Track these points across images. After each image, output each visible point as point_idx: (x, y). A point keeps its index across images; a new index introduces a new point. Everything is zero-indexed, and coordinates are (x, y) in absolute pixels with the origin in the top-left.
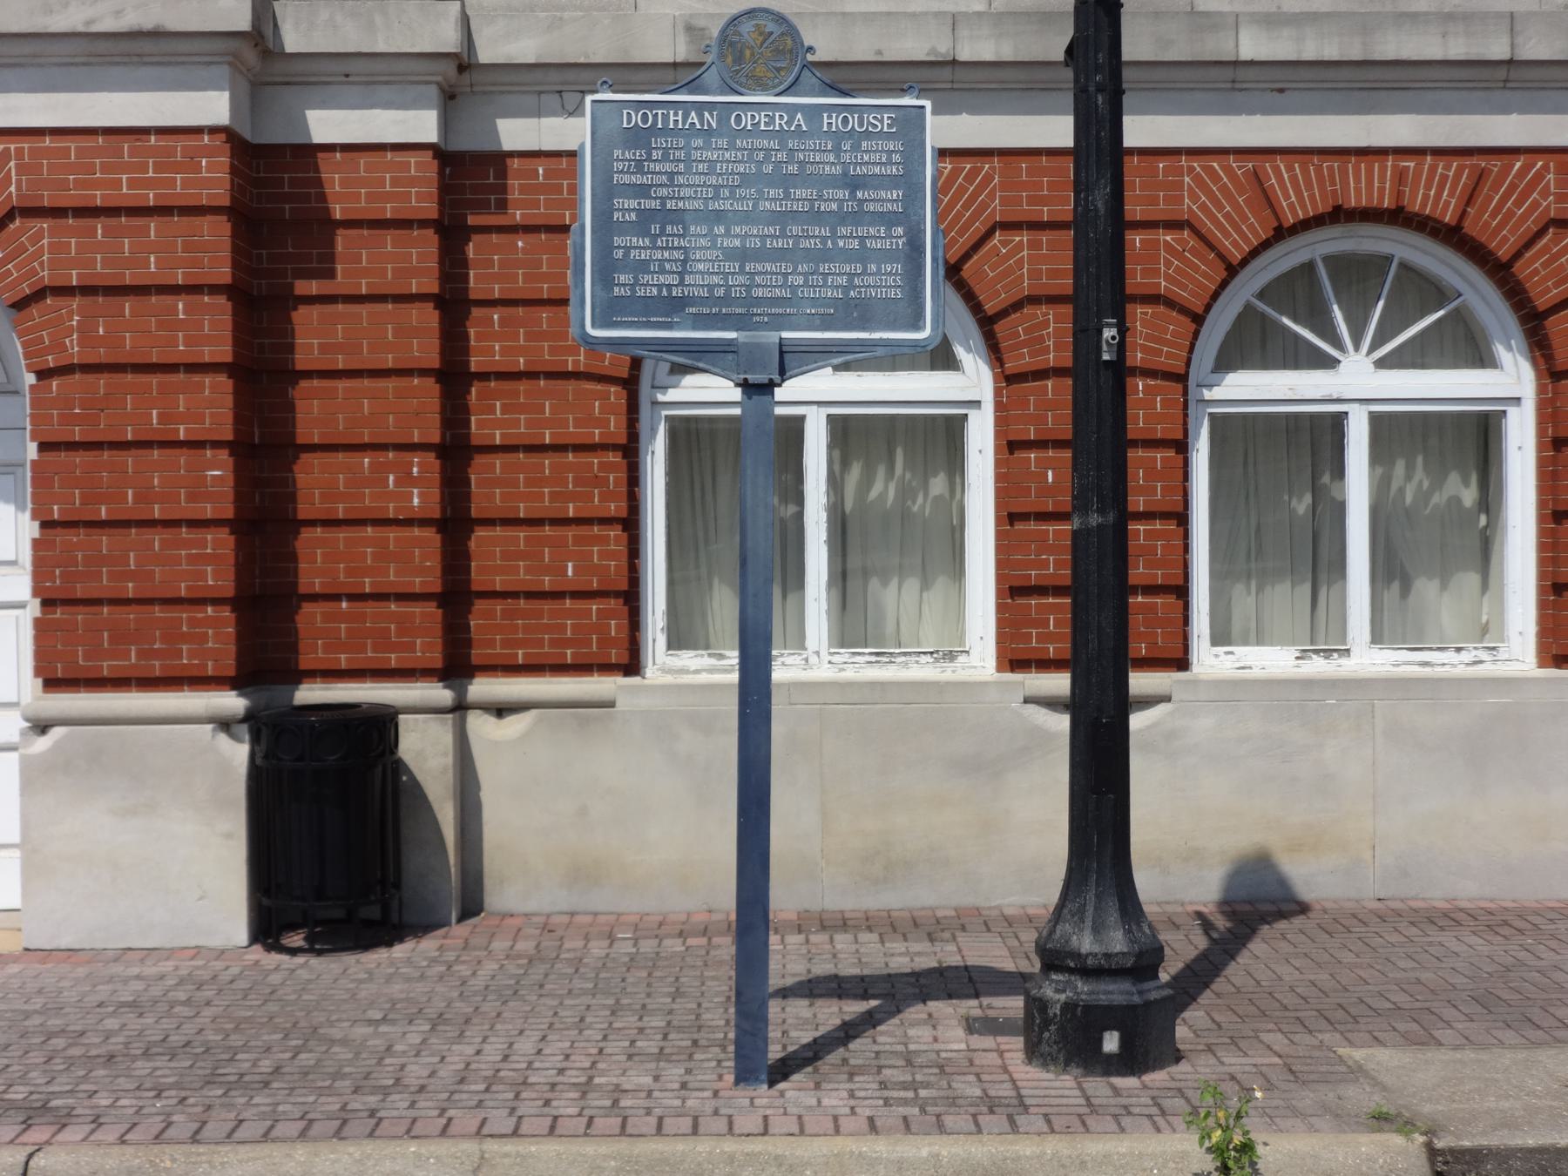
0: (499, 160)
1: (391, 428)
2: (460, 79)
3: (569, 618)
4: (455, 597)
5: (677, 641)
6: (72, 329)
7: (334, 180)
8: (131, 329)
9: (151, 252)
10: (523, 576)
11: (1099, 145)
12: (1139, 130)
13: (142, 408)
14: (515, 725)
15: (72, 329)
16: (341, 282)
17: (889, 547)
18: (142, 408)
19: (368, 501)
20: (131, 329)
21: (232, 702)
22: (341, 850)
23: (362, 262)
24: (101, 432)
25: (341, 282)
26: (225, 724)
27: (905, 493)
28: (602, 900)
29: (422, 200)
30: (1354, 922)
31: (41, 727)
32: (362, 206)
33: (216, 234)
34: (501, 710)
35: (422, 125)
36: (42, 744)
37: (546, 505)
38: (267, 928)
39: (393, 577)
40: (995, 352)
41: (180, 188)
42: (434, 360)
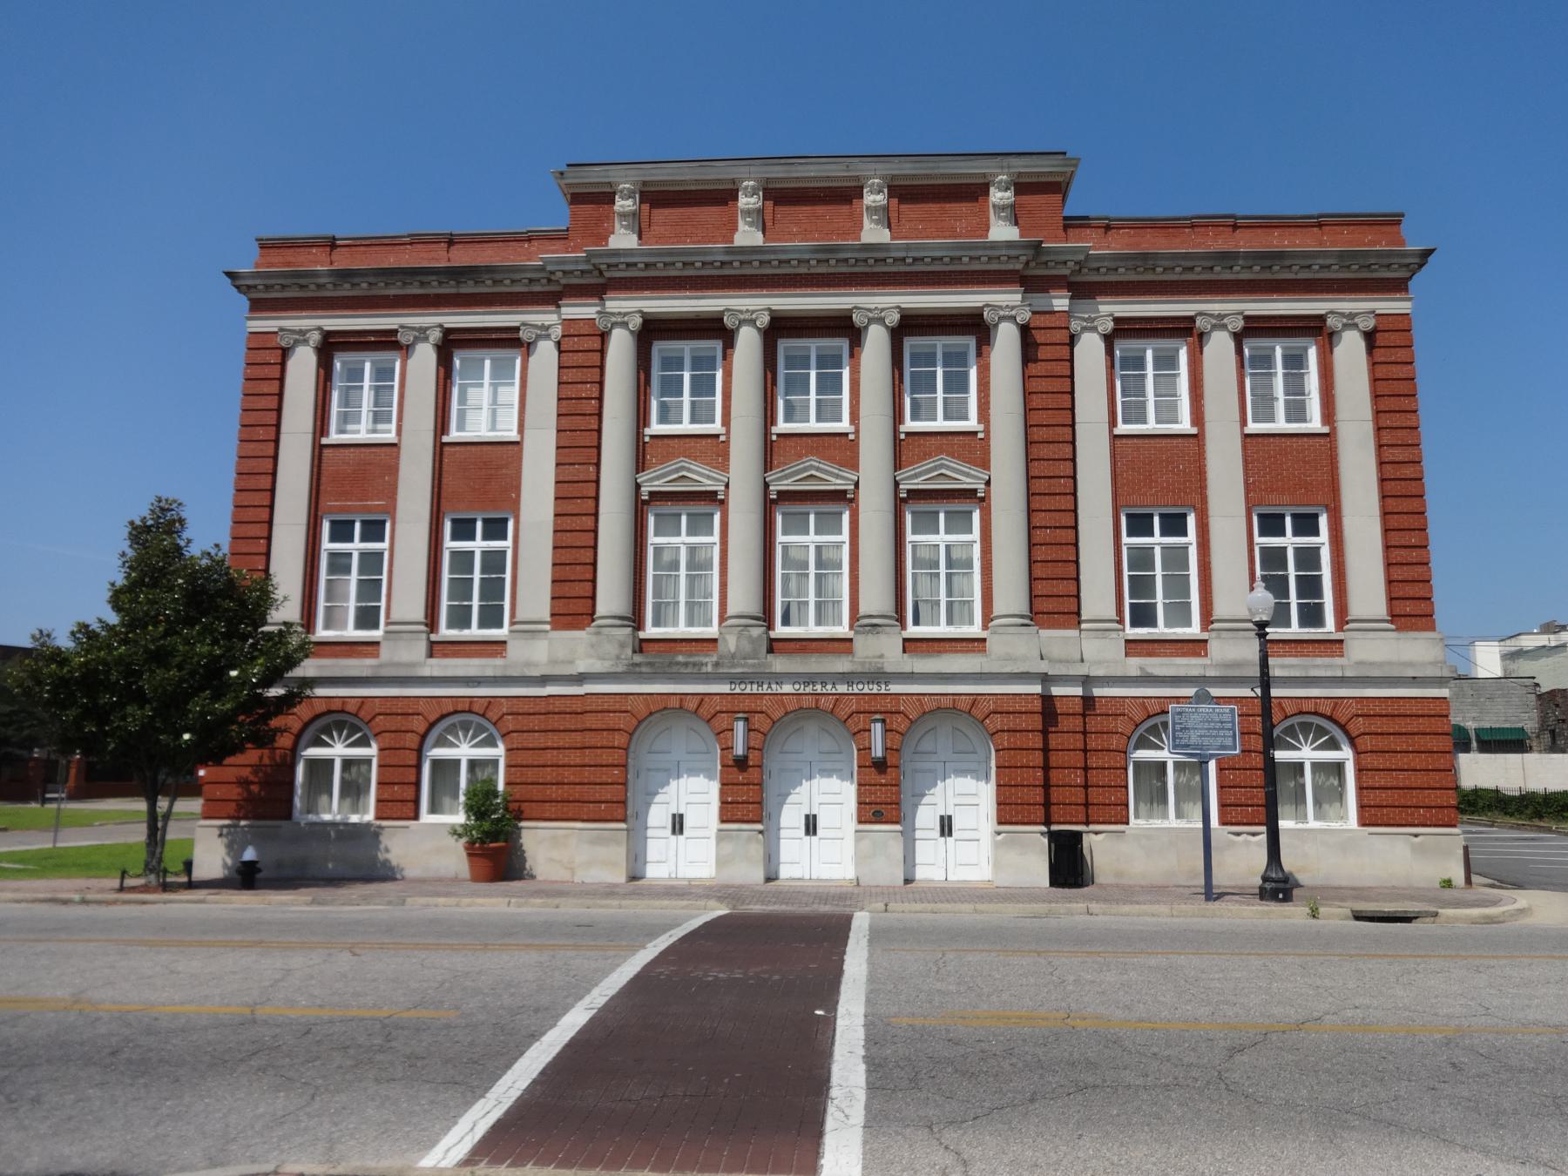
0: (1093, 698)
1: (1072, 763)
2: (1087, 681)
3: (1112, 810)
4: (1047, 804)
5: (1137, 816)
6: (1005, 741)
7: (1058, 704)
8: (1019, 739)
9: (1023, 722)
10: (1101, 800)
11: (1266, 697)
12: (1274, 692)
13: (1023, 758)
14: (1100, 837)
15: (1005, 741)
16: (1060, 728)
17: (1329, 796)
18: (1023, 758)
19: (1067, 781)
20: (1019, 739)
21: (1044, 829)
22: (1069, 867)
23: (1065, 724)
24: (1013, 763)
25: (1060, 728)
26: (1042, 834)
27: (1189, 780)
28: (1124, 881)
29: (1079, 709)
30: (1313, 888)
31: (999, 833)
32: (1064, 710)
33: (1038, 718)
34: (1096, 833)
35: (1078, 691)
36: (999, 838)
37: (1106, 783)
38: (1052, 884)
39: (1073, 799)
40: (1353, 745)
41: (1029, 707)
42: (1041, 745)
